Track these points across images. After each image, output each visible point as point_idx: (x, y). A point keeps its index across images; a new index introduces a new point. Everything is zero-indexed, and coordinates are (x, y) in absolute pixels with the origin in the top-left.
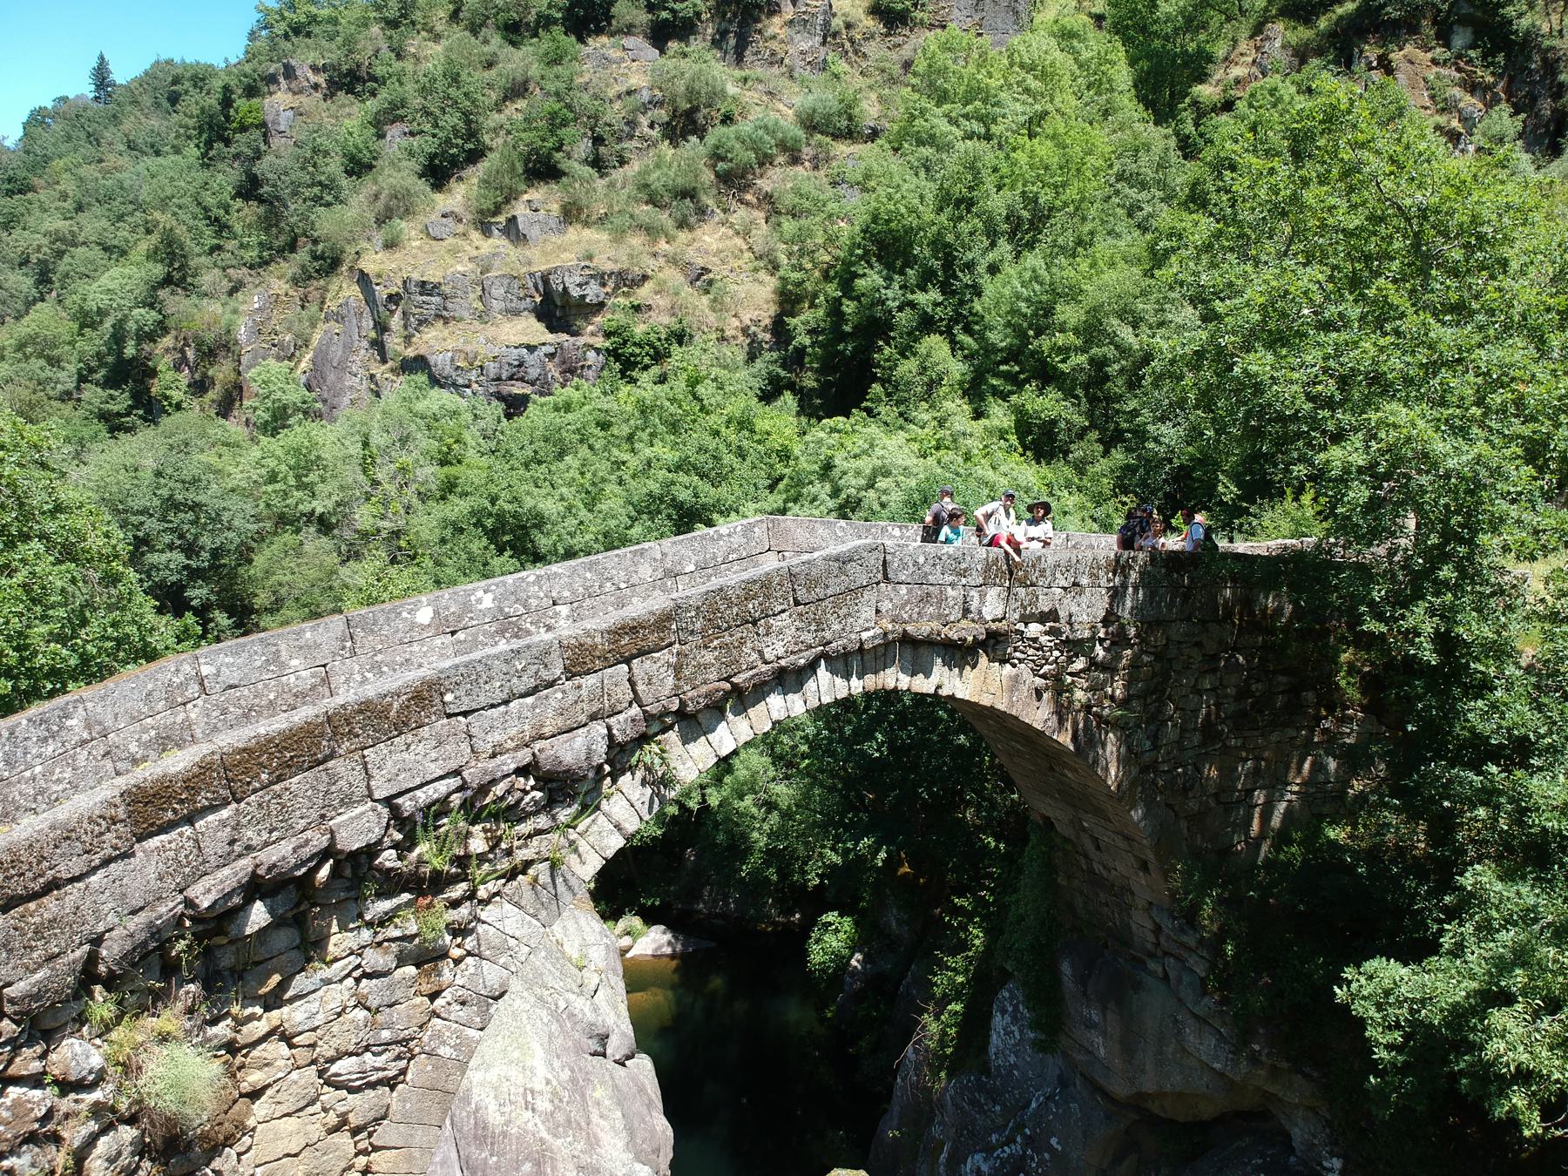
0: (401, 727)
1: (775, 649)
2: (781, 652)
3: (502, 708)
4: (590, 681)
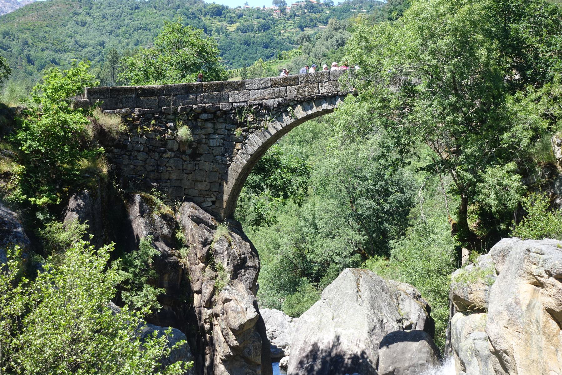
0: (236, 90)
1: (323, 91)
2: (325, 91)
3: (256, 91)
4: (277, 89)
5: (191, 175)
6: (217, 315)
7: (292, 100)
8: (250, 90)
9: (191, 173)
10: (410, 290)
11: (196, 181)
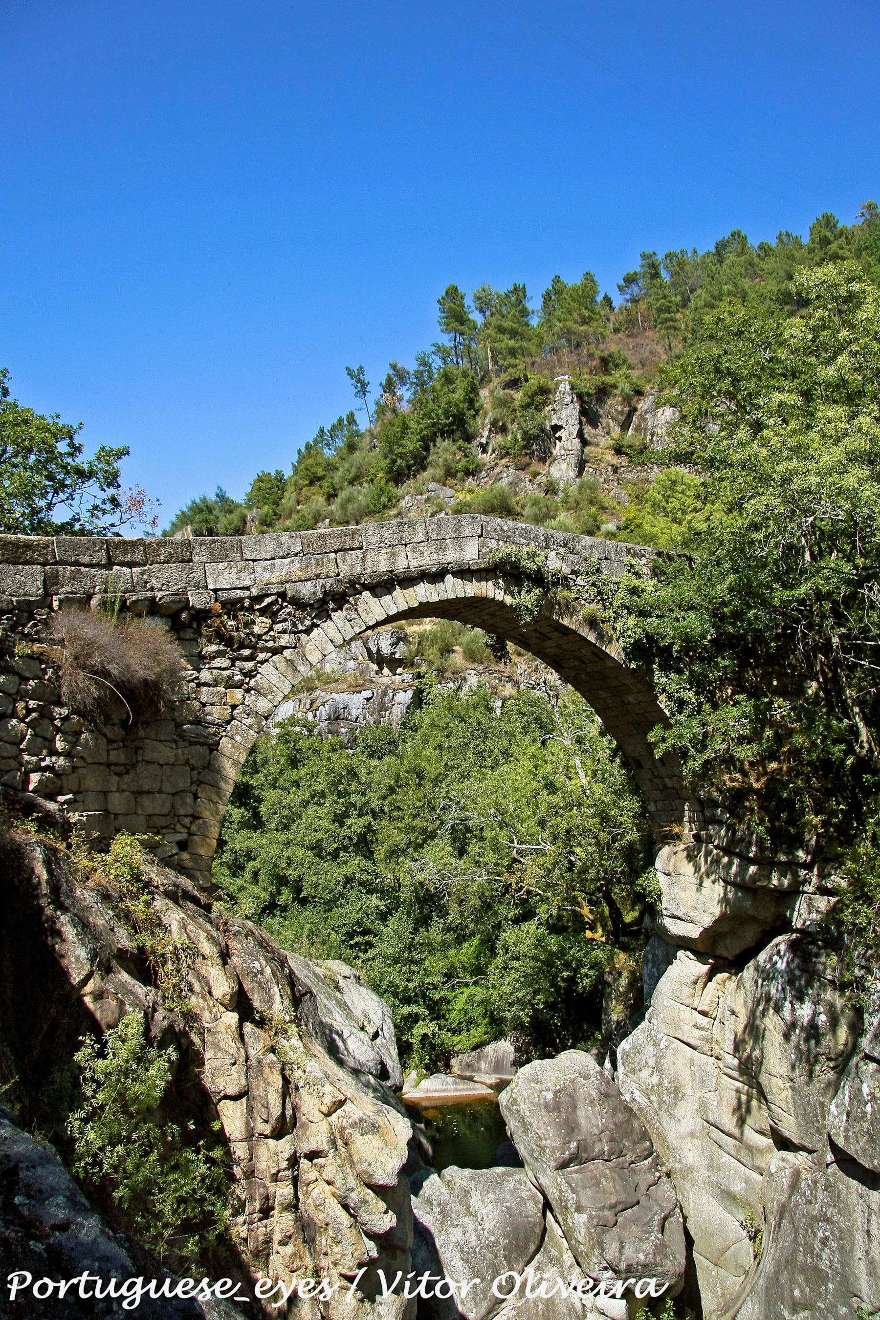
3: (268, 562)
5: (127, 778)
6: (312, 1156)
7: (352, 583)
8: (254, 561)
9: (127, 772)
10: (346, 969)
11: (138, 793)
